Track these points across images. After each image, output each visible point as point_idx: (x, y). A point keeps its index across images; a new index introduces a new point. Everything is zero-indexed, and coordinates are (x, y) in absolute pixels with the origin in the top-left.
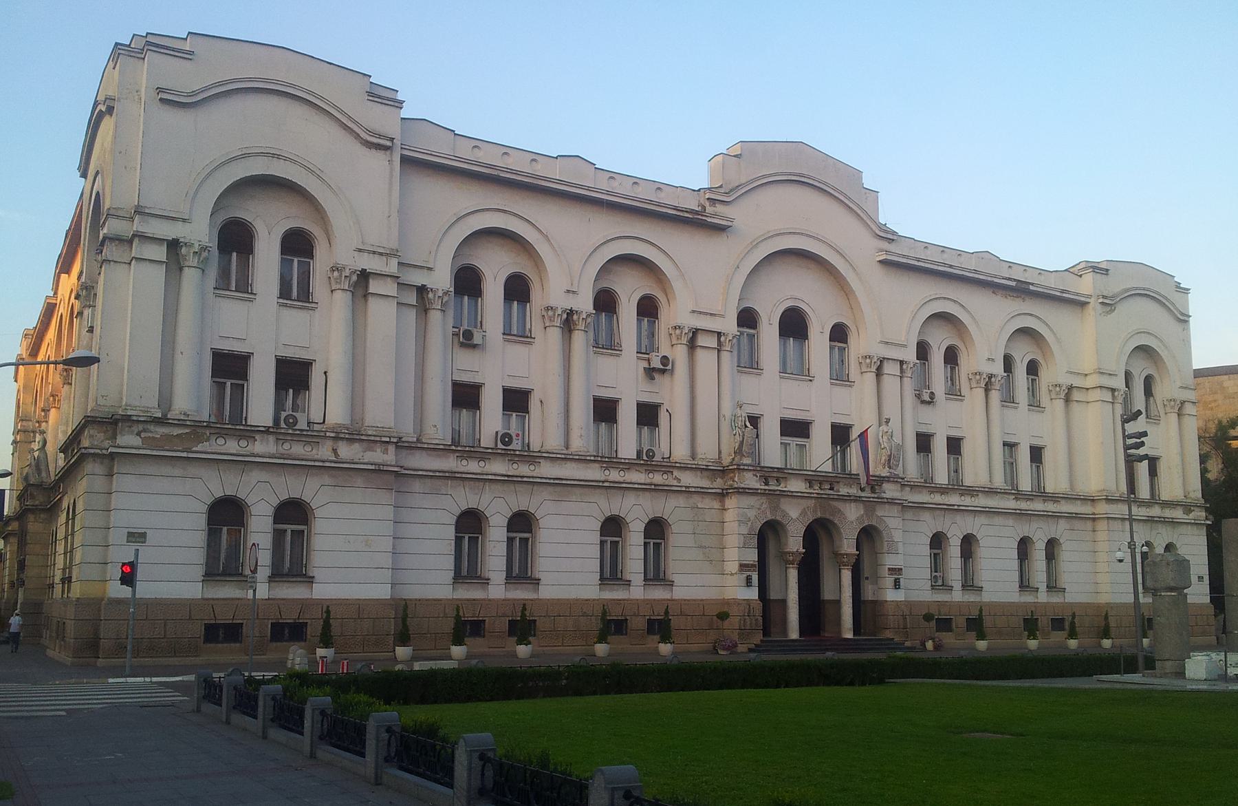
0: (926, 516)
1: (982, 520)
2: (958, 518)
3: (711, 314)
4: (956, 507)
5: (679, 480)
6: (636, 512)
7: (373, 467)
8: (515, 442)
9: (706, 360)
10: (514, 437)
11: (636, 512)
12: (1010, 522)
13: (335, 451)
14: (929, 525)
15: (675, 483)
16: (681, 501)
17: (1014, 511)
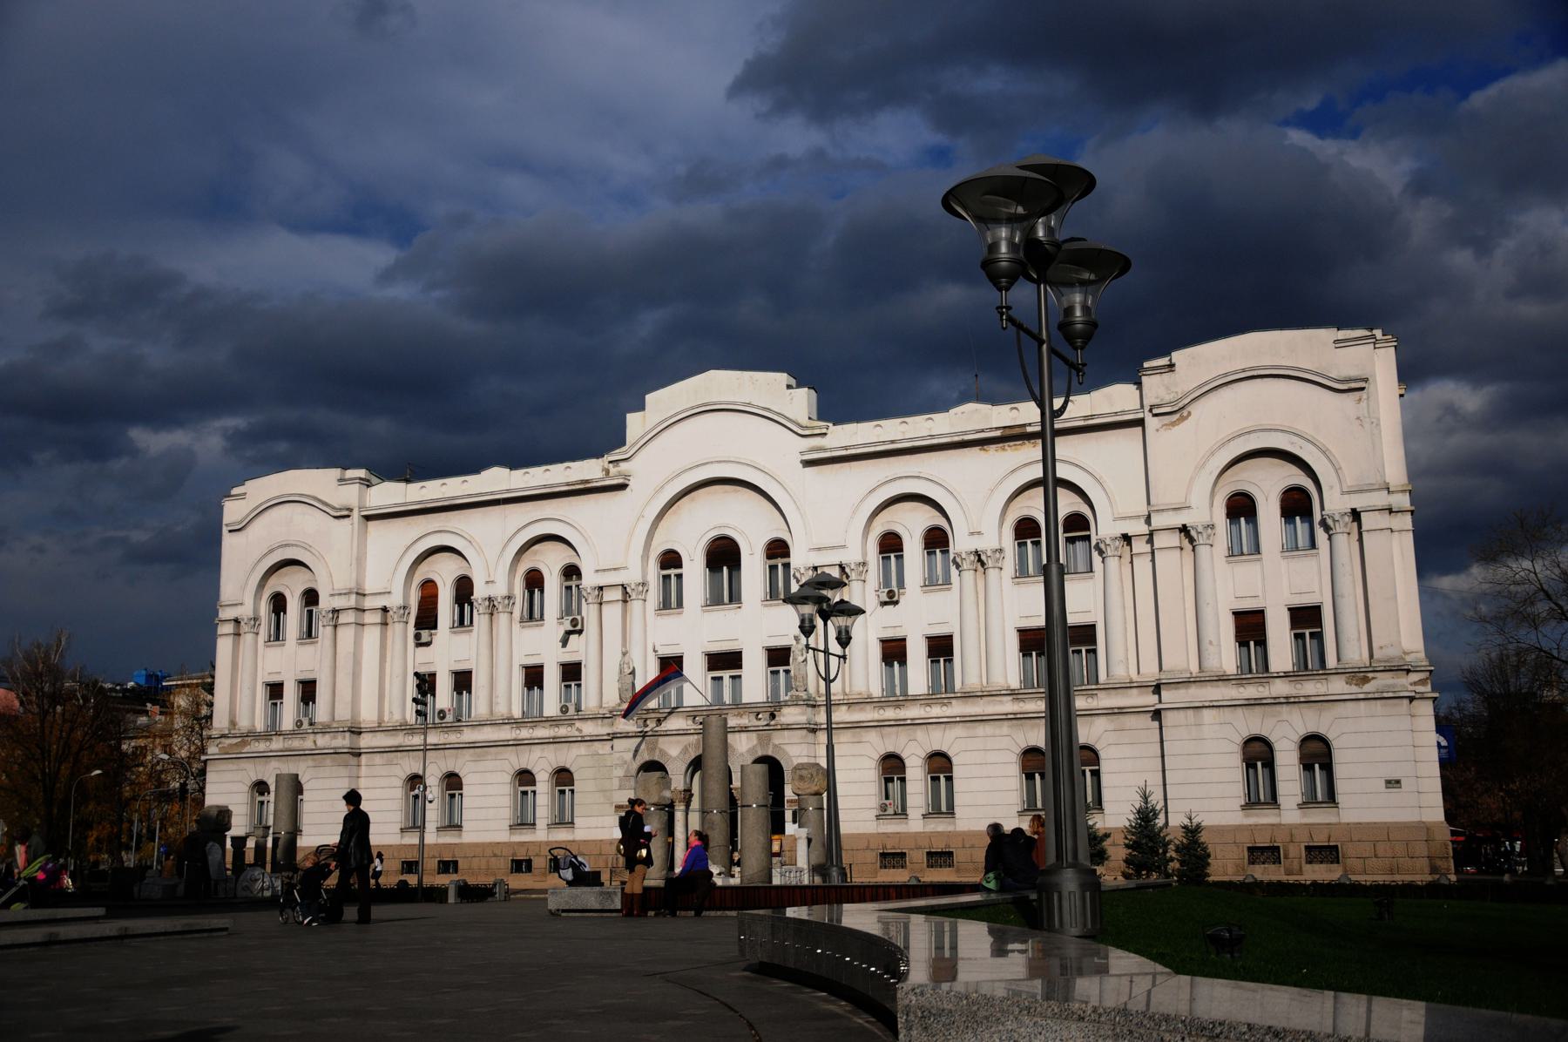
0: (872, 736)
1: (958, 731)
2: (920, 733)
3: (615, 569)
4: (909, 722)
5: (579, 730)
6: (542, 763)
7: (332, 751)
8: (448, 716)
9: (612, 613)
10: (447, 712)
11: (542, 763)
12: (1005, 728)
13: (315, 742)
14: (878, 744)
15: (577, 733)
16: (582, 749)
17: (1004, 717)
